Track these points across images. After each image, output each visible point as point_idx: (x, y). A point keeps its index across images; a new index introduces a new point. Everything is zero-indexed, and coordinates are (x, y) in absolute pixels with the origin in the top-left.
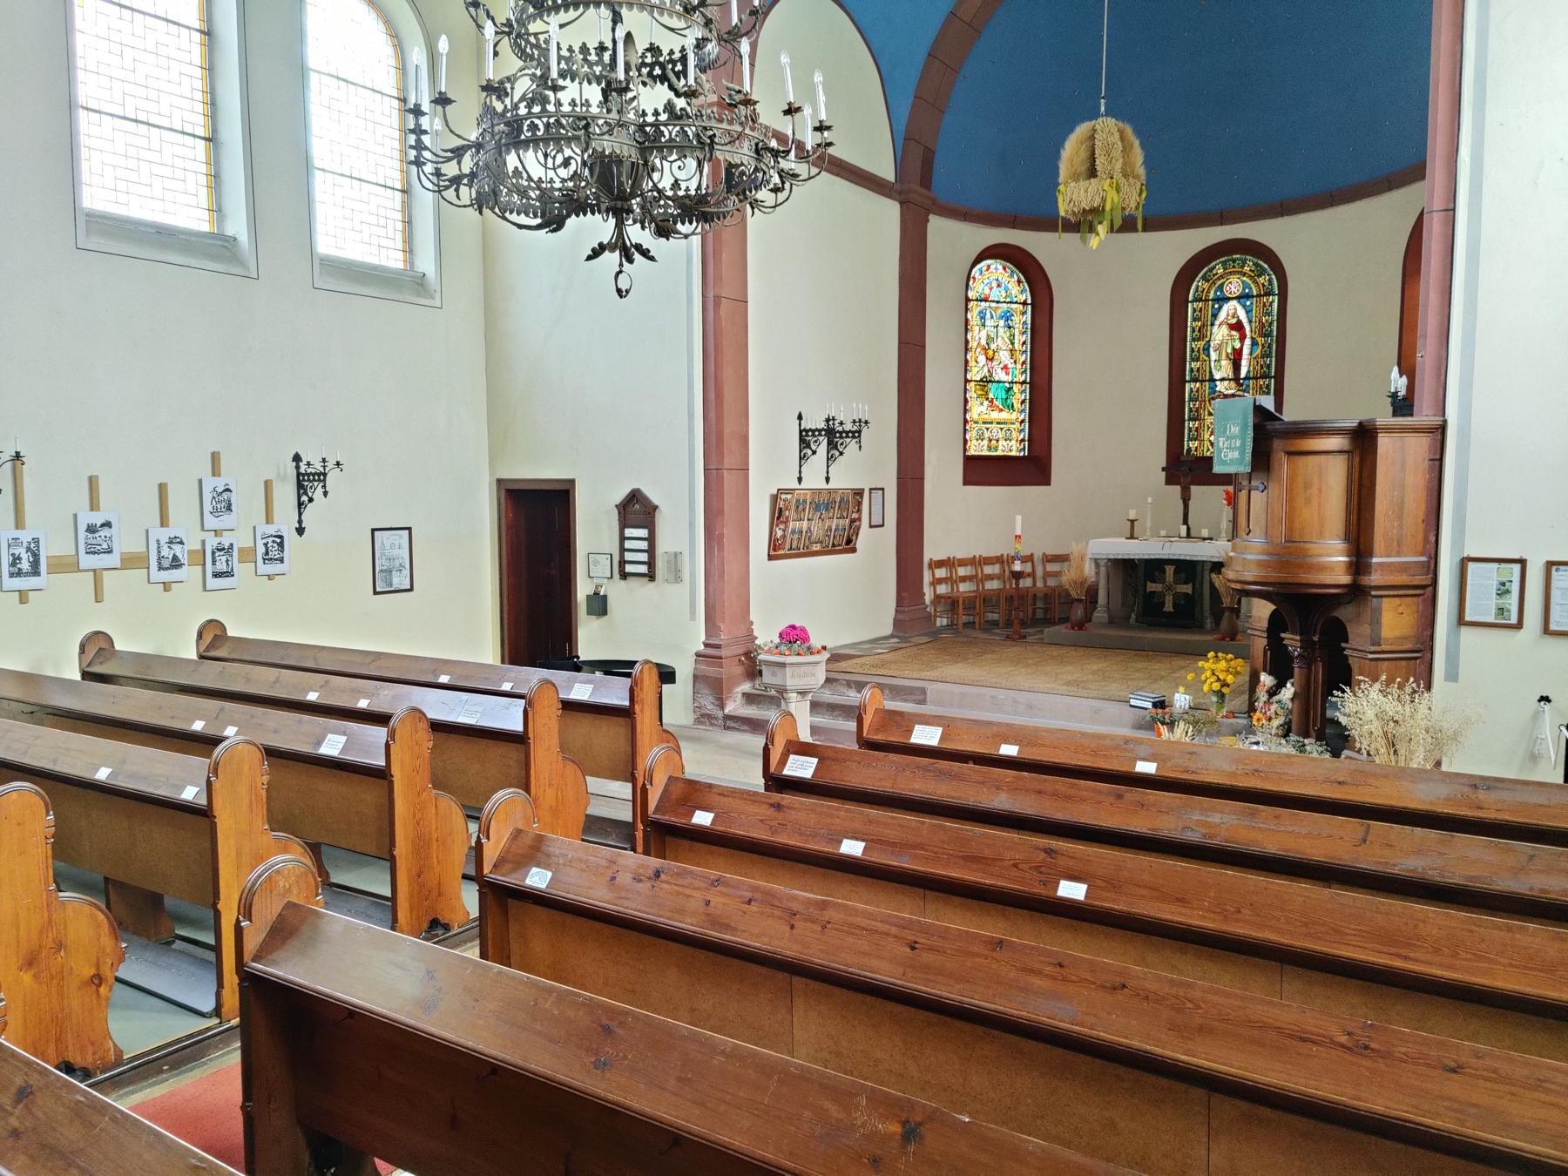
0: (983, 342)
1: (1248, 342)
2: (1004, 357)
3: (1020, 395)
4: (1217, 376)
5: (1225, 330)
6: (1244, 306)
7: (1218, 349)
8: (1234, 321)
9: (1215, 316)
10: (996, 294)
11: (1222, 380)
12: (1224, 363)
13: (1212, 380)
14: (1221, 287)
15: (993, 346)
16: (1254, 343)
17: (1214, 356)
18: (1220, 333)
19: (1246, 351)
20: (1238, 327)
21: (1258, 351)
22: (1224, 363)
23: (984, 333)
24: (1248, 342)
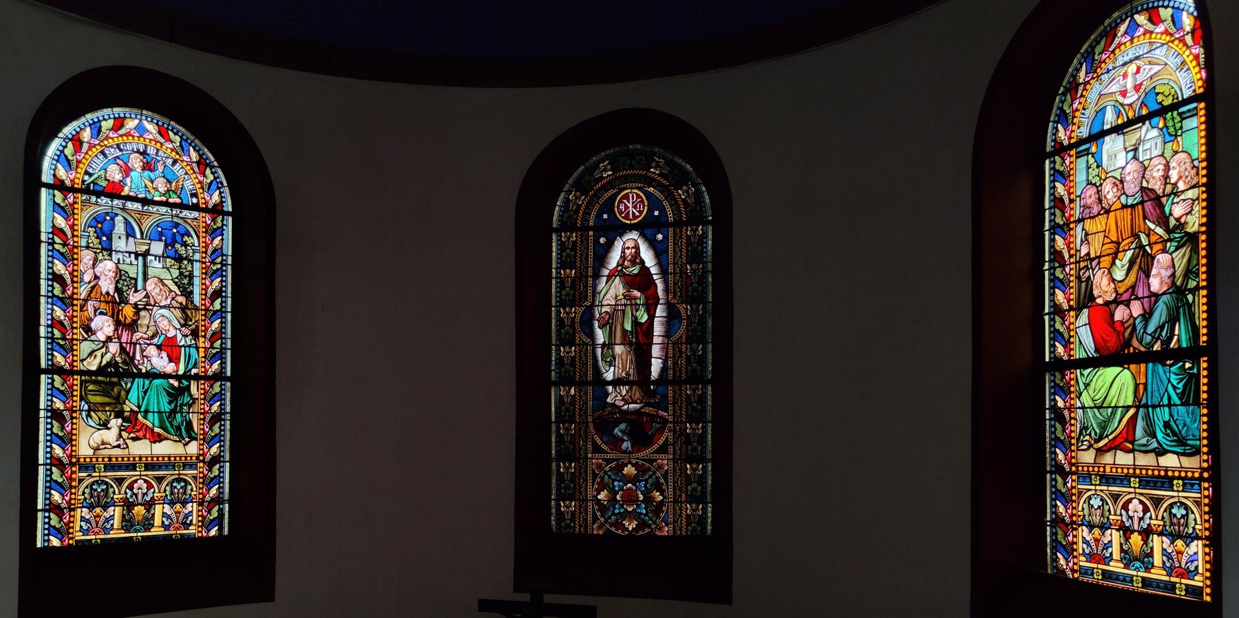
0: (107, 285)
1: (660, 311)
2: (167, 322)
3: (209, 404)
4: (609, 376)
5: (618, 287)
6: (652, 244)
7: (609, 322)
8: (635, 270)
9: (601, 258)
10: (136, 183)
11: (616, 382)
12: (619, 349)
13: (600, 383)
14: (609, 206)
15: (134, 298)
16: (672, 316)
17: (600, 336)
18: (611, 292)
19: (658, 329)
20: (642, 281)
21: (681, 330)
22: (619, 349)
23: (107, 267)
24: (660, 311)
